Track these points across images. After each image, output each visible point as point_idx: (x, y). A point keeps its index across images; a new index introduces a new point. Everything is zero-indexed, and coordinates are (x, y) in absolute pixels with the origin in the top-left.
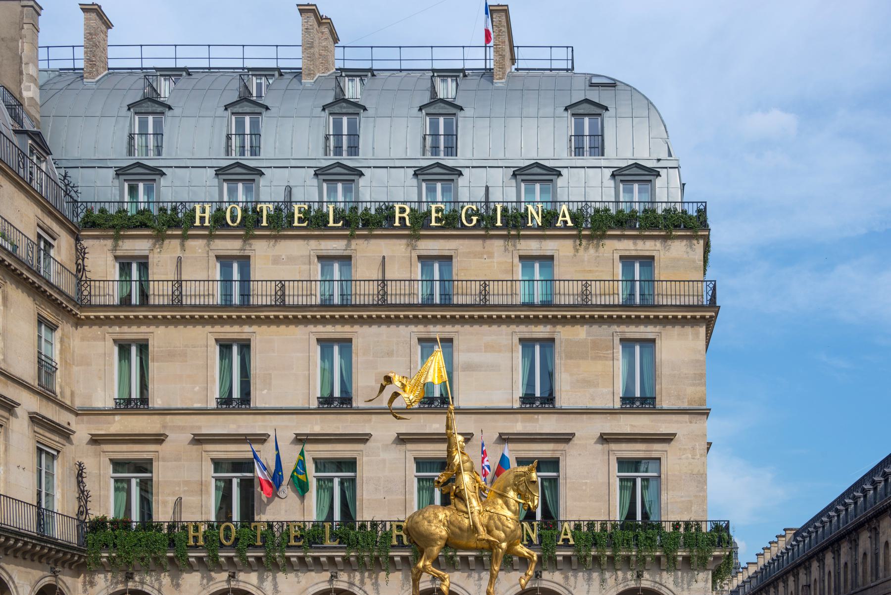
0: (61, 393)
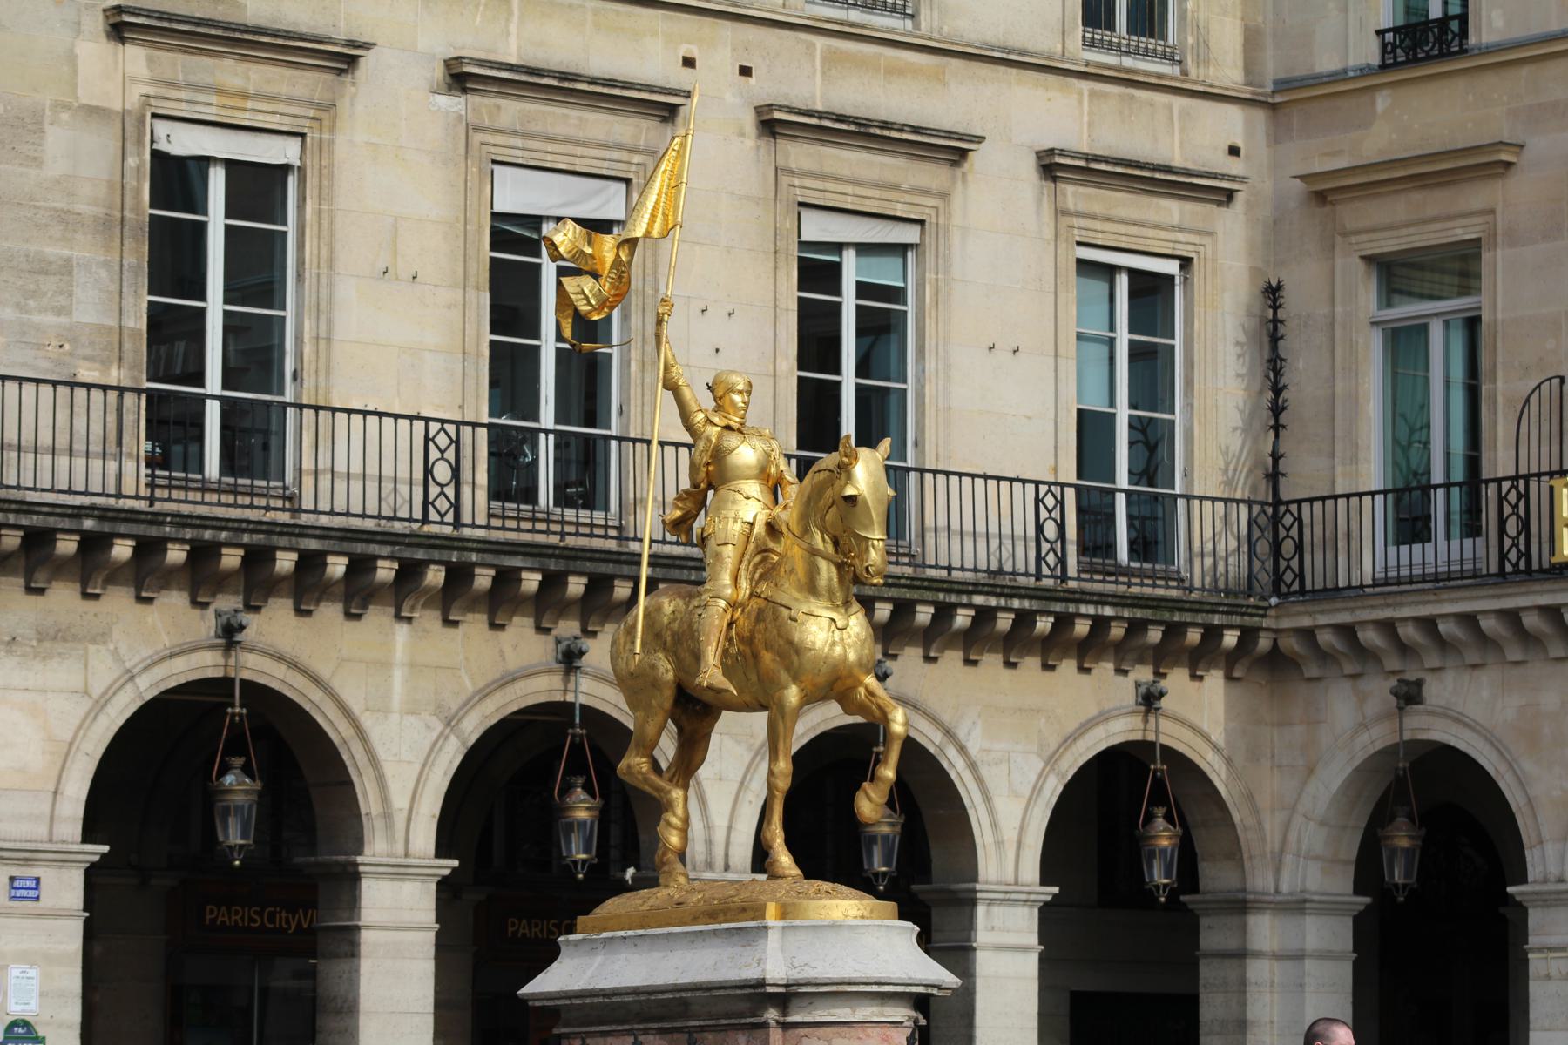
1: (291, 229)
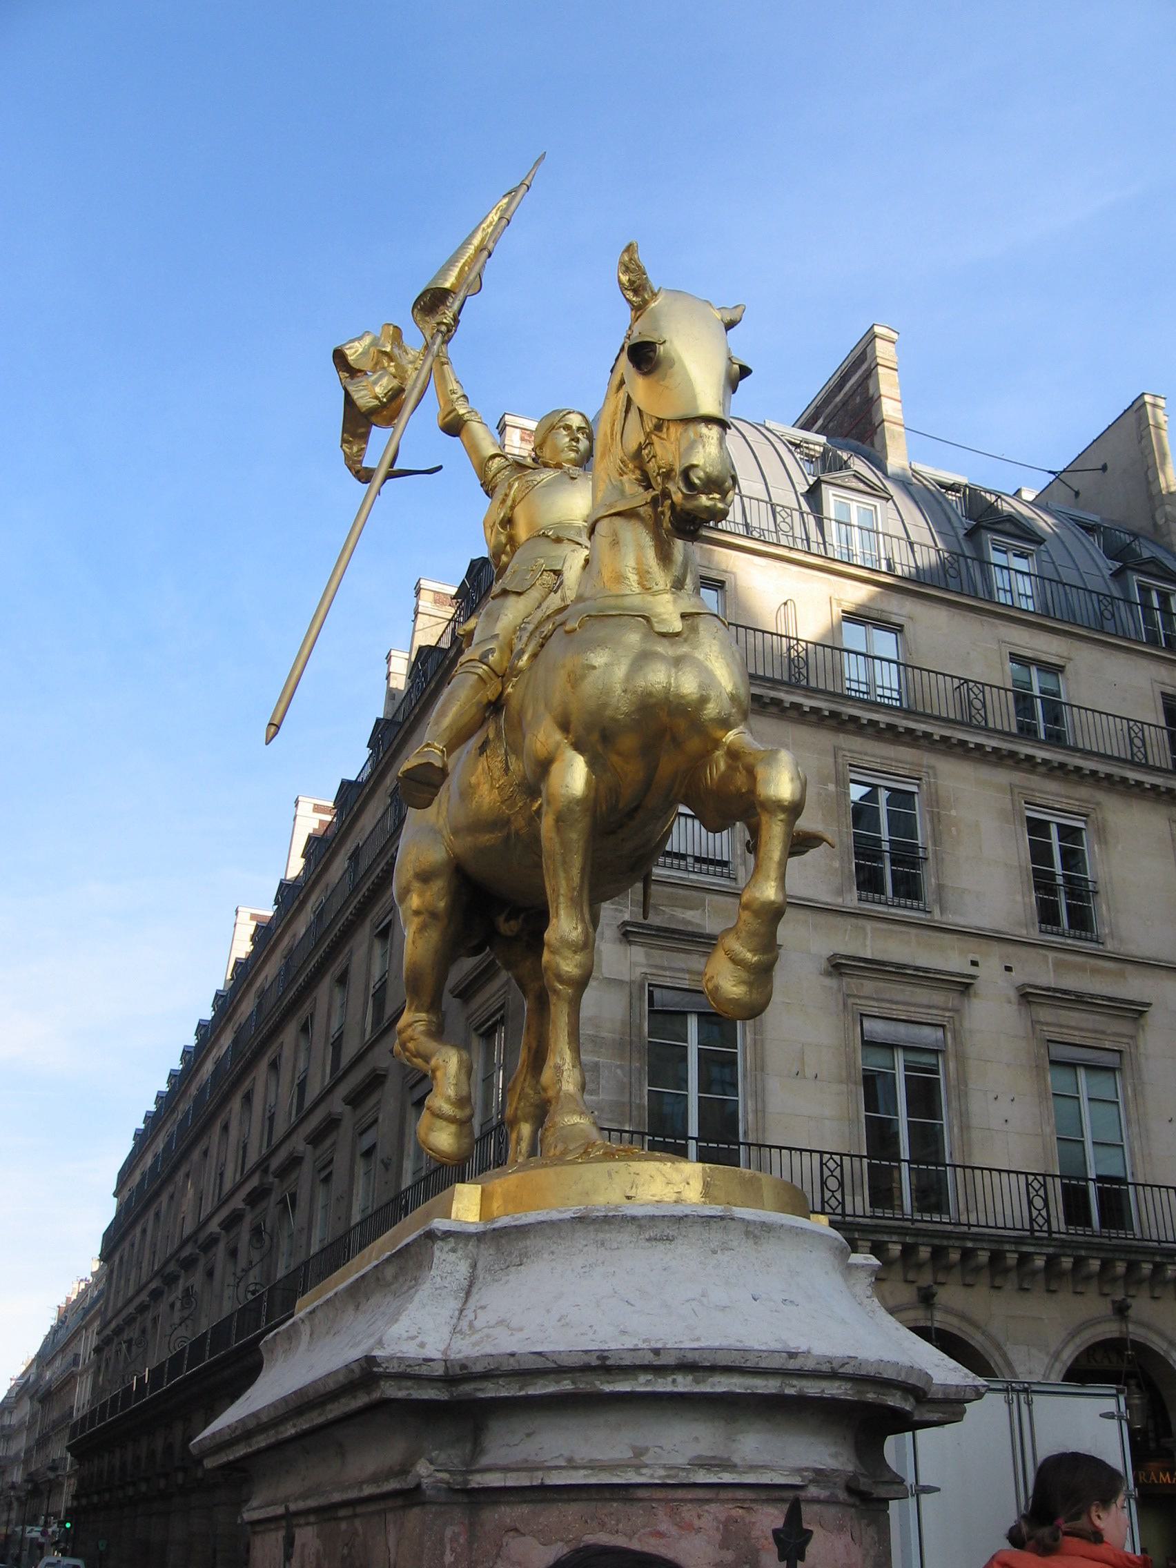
1: (739, 1051)
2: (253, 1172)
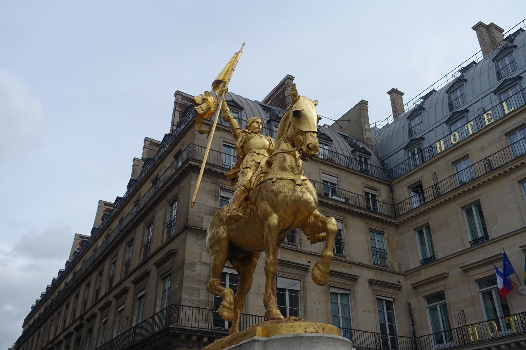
0: (391, 266)
2: (77, 320)
